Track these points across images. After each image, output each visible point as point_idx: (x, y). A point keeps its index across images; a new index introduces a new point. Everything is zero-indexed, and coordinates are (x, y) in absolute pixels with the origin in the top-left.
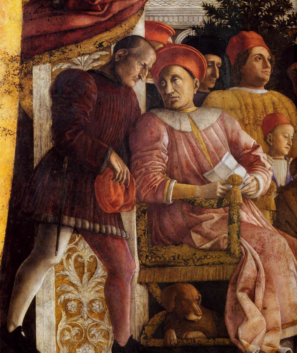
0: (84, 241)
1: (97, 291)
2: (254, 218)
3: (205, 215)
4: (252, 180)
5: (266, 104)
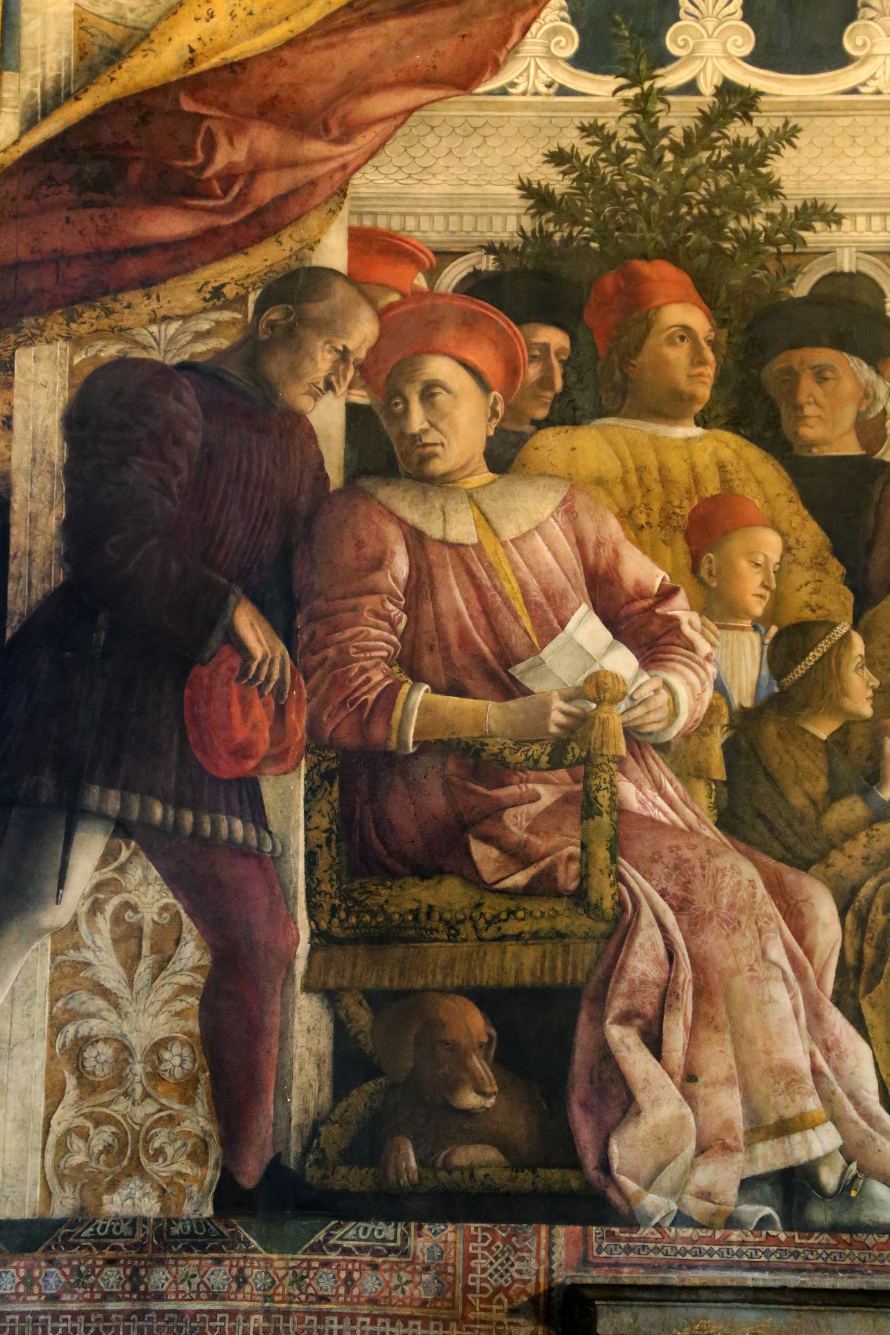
0: (143, 858)
1: (178, 1014)
2: (660, 801)
3: (513, 790)
4: (656, 691)
5: (700, 469)
